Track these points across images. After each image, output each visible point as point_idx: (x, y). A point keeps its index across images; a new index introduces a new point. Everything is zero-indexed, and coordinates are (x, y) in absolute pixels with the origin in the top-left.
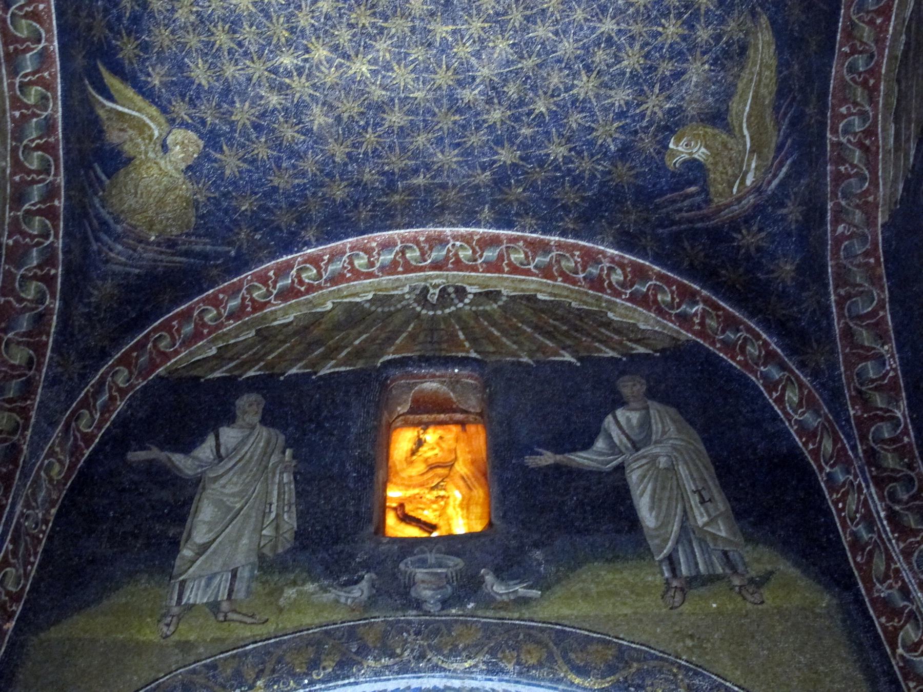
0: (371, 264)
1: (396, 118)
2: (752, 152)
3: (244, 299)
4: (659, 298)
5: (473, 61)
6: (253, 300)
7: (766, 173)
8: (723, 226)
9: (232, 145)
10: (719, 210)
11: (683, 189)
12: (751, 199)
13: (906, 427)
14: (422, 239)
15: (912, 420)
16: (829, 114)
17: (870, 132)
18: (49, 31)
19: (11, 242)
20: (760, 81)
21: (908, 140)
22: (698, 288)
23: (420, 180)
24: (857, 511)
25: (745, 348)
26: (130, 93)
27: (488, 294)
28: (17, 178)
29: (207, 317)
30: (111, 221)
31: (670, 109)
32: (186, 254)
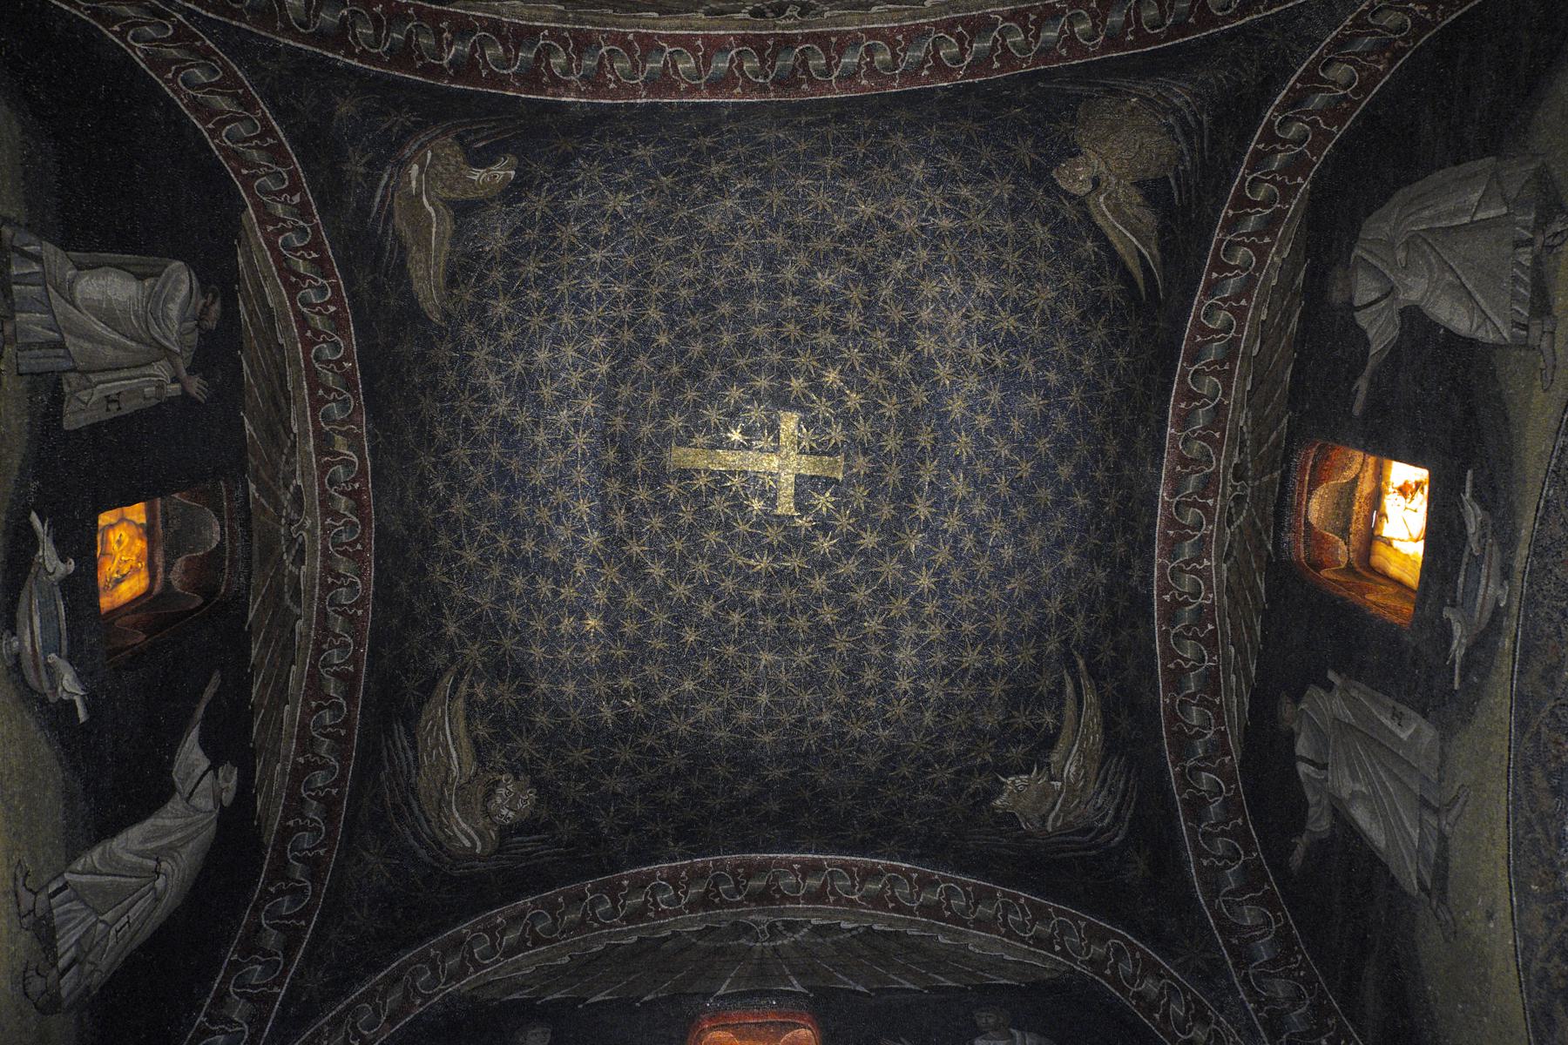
0: (870, 51)
1: (829, 163)
2: (419, 195)
3: (1036, 37)
5: (743, 212)
6: (1026, 31)
8: (435, 123)
9: (1019, 164)
10: (445, 133)
12: (407, 153)
14: (805, 86)
17: (293, 289)
18: (1183, 381)
19: (1300, 180)
23: (804, 120)
26: (1119, 247)
27: (722, 12)
28: (1267, 240)
29: (1084, 27)
30: (1177, 130)
31: (520, 201)
32: (1097, 84)
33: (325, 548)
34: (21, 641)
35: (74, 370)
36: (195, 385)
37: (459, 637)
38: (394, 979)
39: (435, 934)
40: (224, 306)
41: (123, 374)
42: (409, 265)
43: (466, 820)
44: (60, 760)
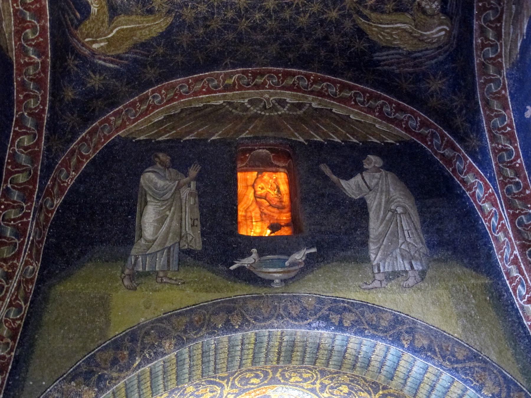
2: (108, 40)
4: (27, 30)
7: (103, 54)
8: (71, 44)
10: (74, 36)
11: (76, 9)
12: (87, 52)
13: (54, 210)
15: (58, 211)
16: (159, 86)
17: (155, 107)
20: (141, 29)
21: (166, 131)
22: (50, 56)
24: (15, 220)
25: (30, 98)
33: (279, 89)
34: (277, 278)
35: (179, 243)
36: (193, 172)
37: (339, 10)
38: (487, 104)
39: (474, 76)
40: (161, 151)
41: (183, 217)
42: (143, 41)
43: (432, 29)
44: (328, 263)
